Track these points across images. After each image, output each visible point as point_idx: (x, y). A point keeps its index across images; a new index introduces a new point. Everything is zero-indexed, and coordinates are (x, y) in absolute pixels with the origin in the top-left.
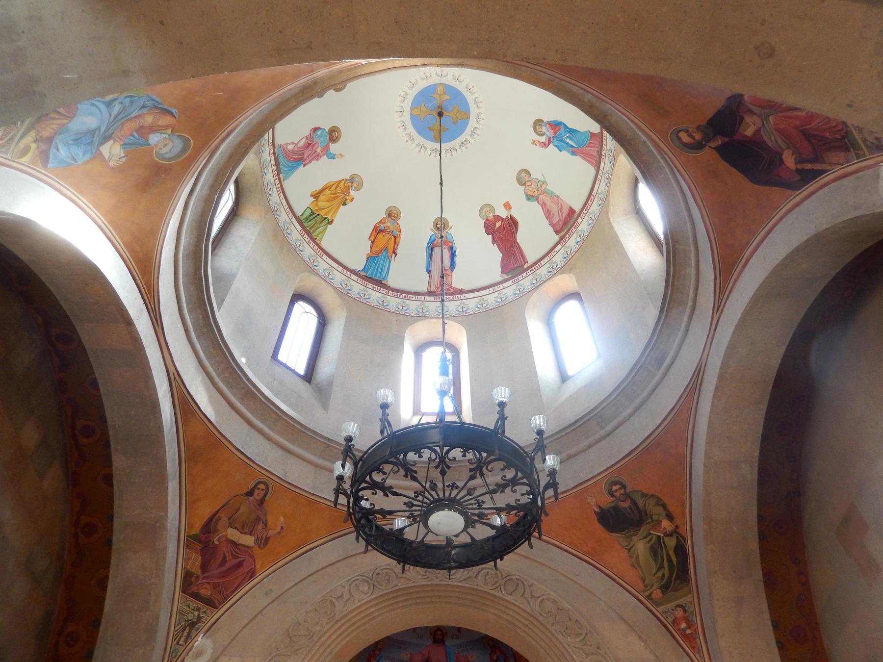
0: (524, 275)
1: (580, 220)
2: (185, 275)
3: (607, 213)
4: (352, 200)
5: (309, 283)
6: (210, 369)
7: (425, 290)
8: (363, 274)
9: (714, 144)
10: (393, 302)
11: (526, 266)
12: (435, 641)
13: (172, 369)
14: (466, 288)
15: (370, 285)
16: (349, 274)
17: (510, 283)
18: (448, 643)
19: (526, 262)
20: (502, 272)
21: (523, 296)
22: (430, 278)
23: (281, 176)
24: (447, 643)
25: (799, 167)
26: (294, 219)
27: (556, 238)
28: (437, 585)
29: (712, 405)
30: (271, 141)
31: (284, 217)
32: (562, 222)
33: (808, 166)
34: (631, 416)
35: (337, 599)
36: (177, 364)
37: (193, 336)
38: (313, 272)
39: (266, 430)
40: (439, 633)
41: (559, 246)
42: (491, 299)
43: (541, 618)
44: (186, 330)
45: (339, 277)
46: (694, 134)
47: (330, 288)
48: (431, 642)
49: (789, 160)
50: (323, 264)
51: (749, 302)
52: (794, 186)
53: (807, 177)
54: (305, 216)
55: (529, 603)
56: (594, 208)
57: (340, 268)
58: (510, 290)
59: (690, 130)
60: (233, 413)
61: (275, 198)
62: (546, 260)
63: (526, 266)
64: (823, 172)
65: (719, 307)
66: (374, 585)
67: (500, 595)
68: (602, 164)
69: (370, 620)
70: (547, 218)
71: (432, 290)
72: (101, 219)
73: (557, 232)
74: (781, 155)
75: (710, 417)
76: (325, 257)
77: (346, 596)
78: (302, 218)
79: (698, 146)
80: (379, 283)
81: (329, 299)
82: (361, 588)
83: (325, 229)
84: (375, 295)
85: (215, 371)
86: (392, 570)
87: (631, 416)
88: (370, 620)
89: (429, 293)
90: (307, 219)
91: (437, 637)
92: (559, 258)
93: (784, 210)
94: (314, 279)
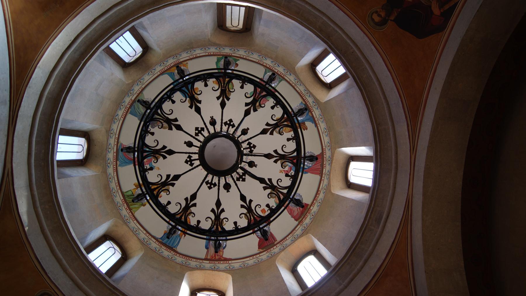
0: (275, 247)
1: (311, 208)
2: (43, 113)
3: (330, 191)
4: (161, 196)
5: (122, 231)
6: (36, 193)
7: (203, 257)
8: (160, 240)
9: (392, 18)
10: (179, 259)
11: (276, 243)
13: (8, 165)
14: (233, 258)
15: (164, 248)
16: (150, 237)
17: (265, 253)
19: (275, 240)
20: (259, 248)
21: (273, 257)
22: (208, 252)
23: (118, 162)
25: (442, 11)
26: (119, 191)
27: (297, 222)
29: (423, 220)
30: (117, 136)
31: (113, 185)
32: (300, 214)
33: (447, 7)
34: (362, 267)
36: (14, 165)
37: (34, 139)
38: (126, 223)
39: (64, 262)
41: (299, 226)
42: (251, 262)
44: (29, 154)
45: (142, 235)
46: (381, 13)
47: (135, 238)
49: (436, 11)
50: (133, 224)
51: (433, 125)
52: (441, 28)
53: (447, 15)
54: (127, 194)
56: (321, 196)
57: (145, 232)
58: (264, 256)
59: (378, 10)
60: (42, 236)
61: (111, 170)
62: (289, 236)
63: (276, 243)
64: (456, 4)
65: (413, 149)
68: (324, 170)
70: (290, 214)
71: (209, 257)
72: (9, 15)
73: (296, 220)
74: (430, 7)
75: (423, 230)
76: (135, 221)
78: (125, 194)
79: (383, 22)
80: (171, 248)
81: (133, 245)
83: (139, 208)
84: (166, 253)
85: (39, 200)
87: (362, 267)
89: (206, 259)
90: (128, 196)
92: (299, 231)
93: (440, 51)
94: (125, 228)
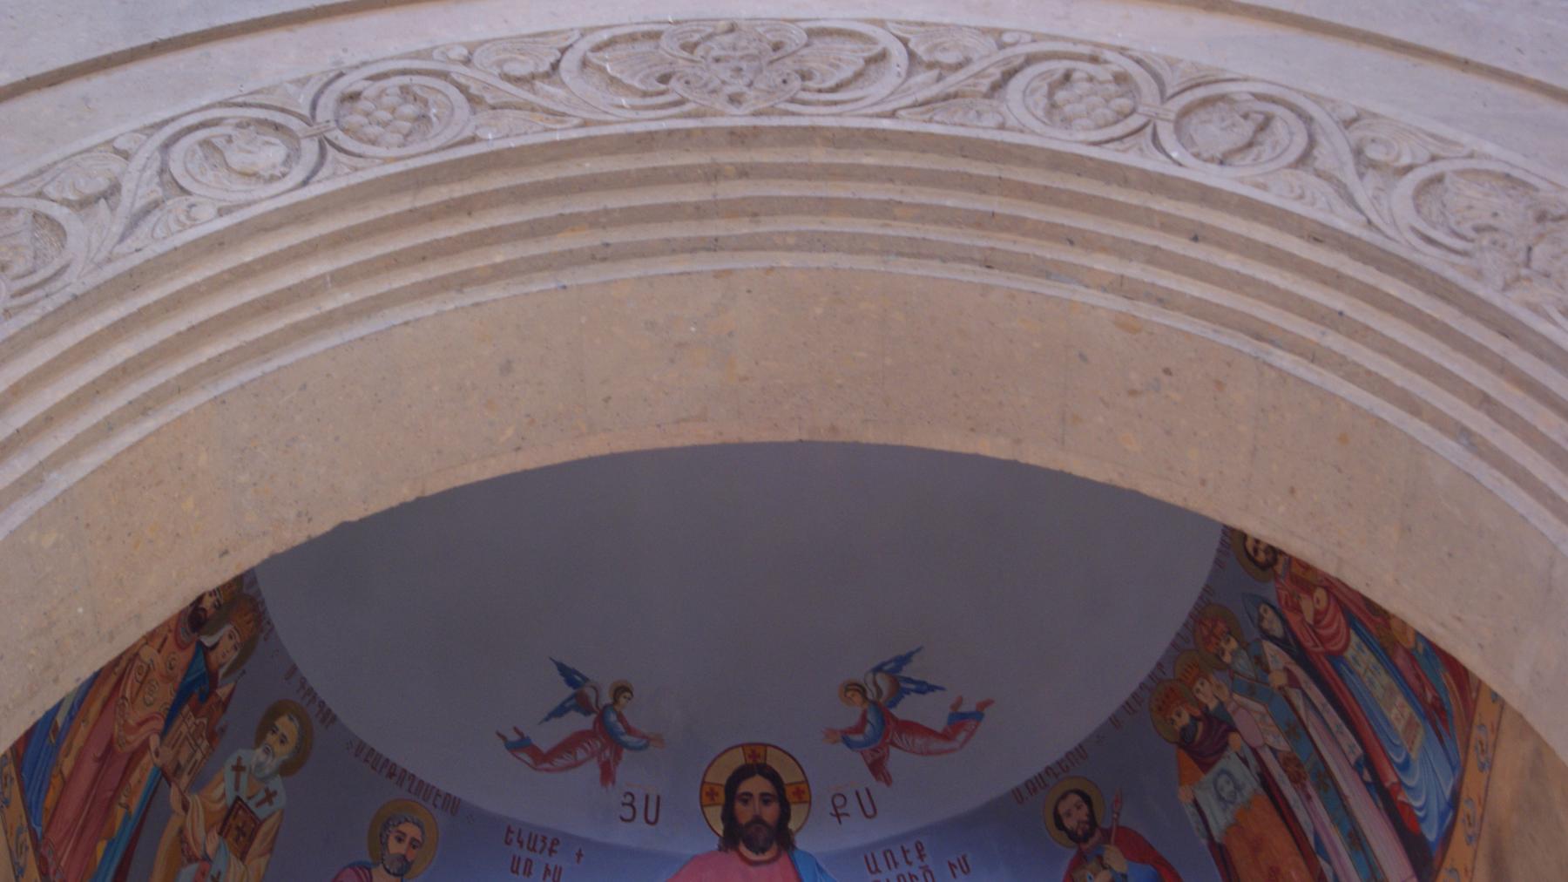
12: (734, 835)
18: (815, 837)
24: (802, 842)
28: (737, 137)
35: (85, 204)
40: (756, 785)
43: (1430, 259)
48: (713, 844)
55: (1350, 200)
66: (324, 144)
67: (1154, 163)
69: (301, 331)
77: (139, 187)
82: (236, 159)
86: (444, 75)
88: (301, 331)
91: (744, 813)
